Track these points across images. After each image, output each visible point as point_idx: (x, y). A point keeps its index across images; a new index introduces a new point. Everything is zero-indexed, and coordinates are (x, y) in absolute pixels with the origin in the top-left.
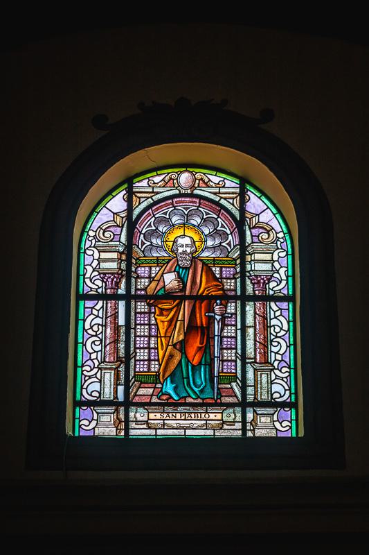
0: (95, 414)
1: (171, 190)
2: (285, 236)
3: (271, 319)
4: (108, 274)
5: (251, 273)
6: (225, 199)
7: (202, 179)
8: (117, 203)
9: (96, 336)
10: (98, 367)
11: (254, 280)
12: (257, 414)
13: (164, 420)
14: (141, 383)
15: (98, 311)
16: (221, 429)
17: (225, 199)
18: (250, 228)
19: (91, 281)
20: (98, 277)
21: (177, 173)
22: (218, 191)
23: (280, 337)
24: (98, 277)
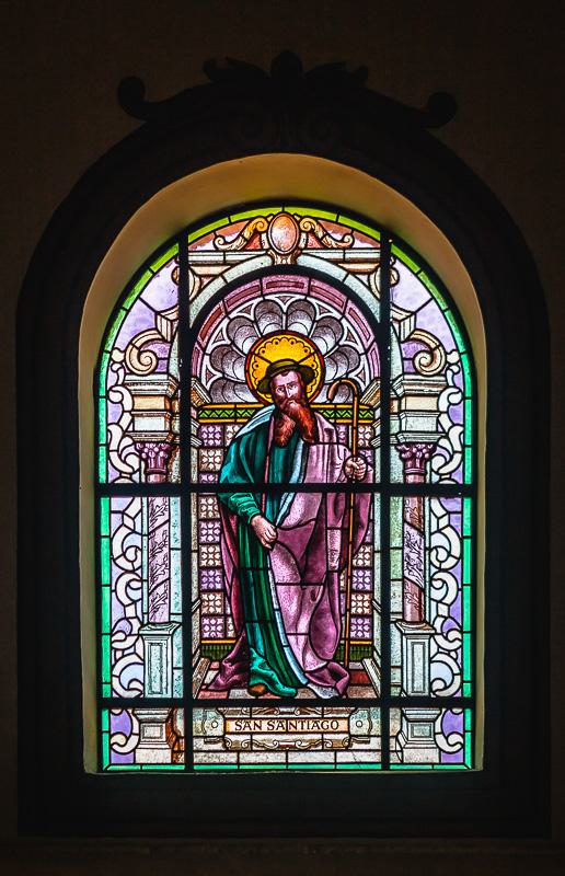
0: (136, 723)
1: (259, 256)
2: (460, 360)
3: (431, 534)
4: (150, 442)
5: (400, 437)
6: (354, 273)
7: (312, 232)
8: (159, 289)
11: (405, 452)
16: (347, 749)
17: (354, 273)
18: (400, 342)
19: (120, 456)
20: (132, 449)
21: (265, 218)
22: (338, 255)
23: (446, 571)
24: (132, 449)
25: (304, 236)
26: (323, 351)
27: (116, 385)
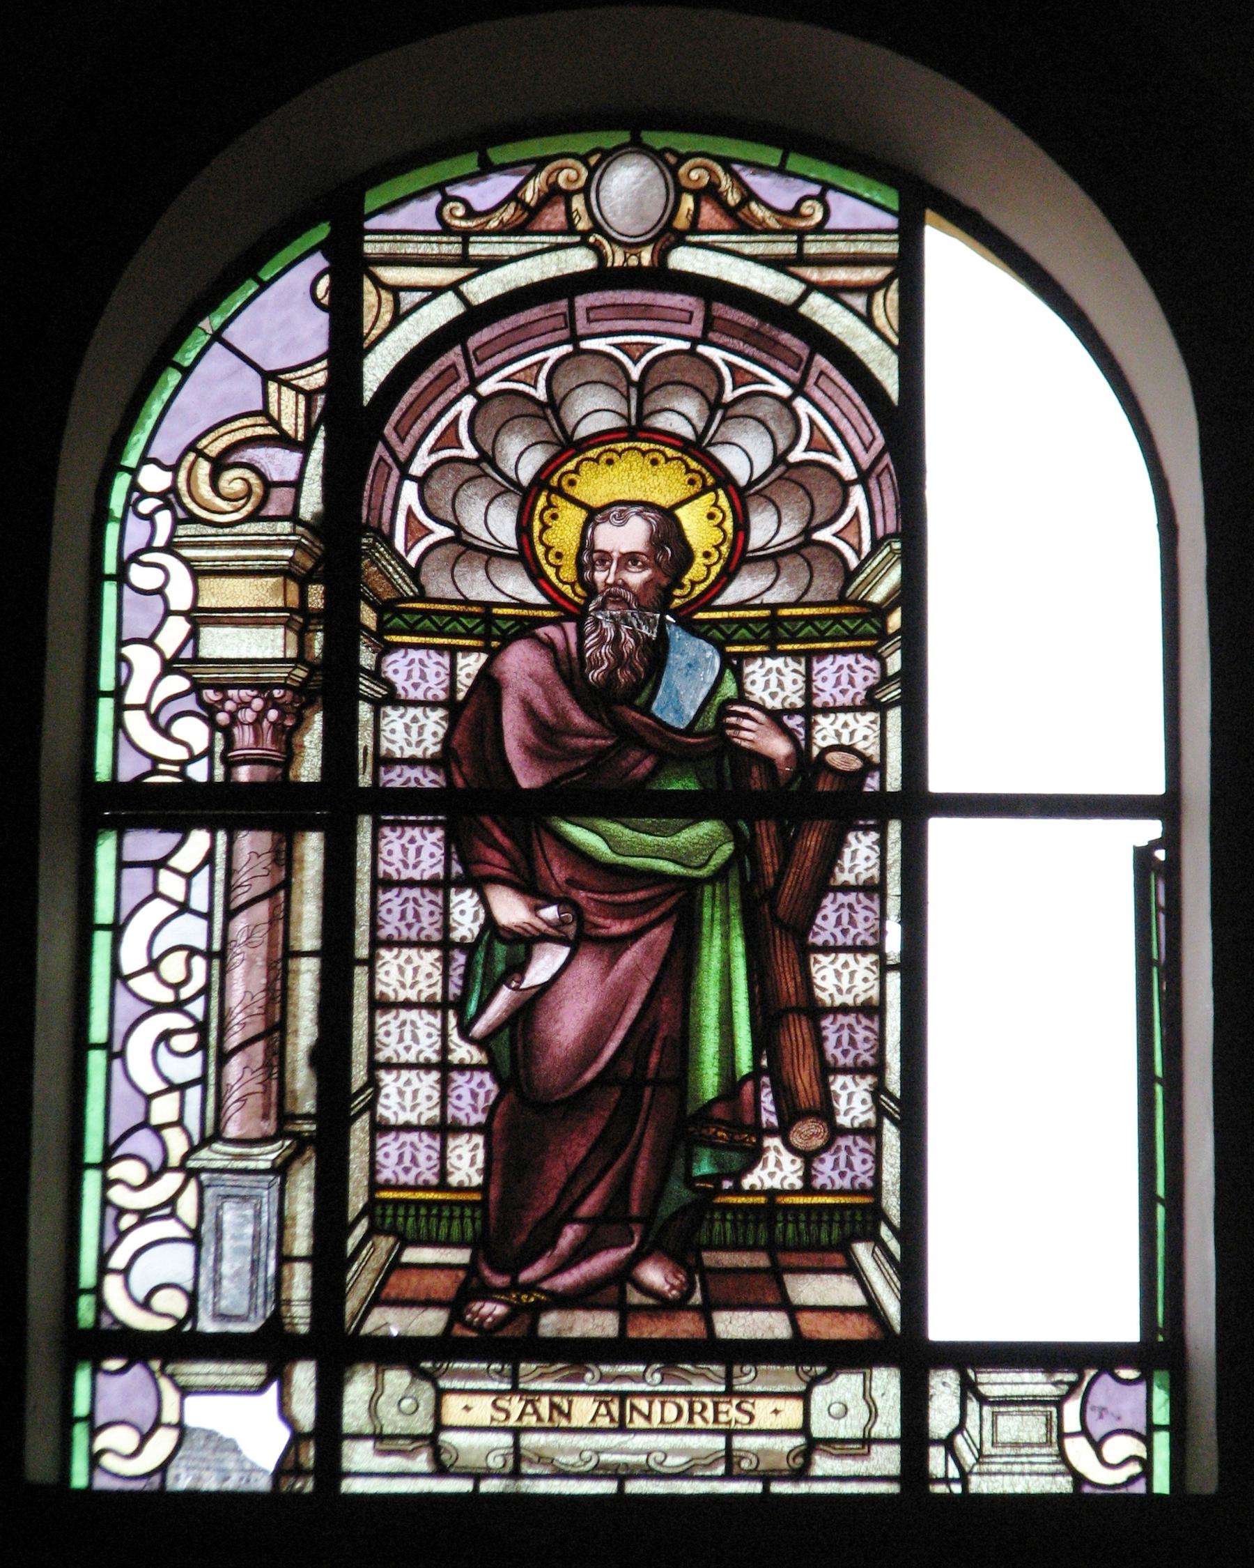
9: (177, 1006)
10: (181, 1168)
12: (983, 1400)
13: (517, 1432)
14: (405, 1242)
15: (189, 877)
19: (153, 719)
24: (190, 703)
25: (688, 203)
26: (742, 476)
27: (149, 548)
